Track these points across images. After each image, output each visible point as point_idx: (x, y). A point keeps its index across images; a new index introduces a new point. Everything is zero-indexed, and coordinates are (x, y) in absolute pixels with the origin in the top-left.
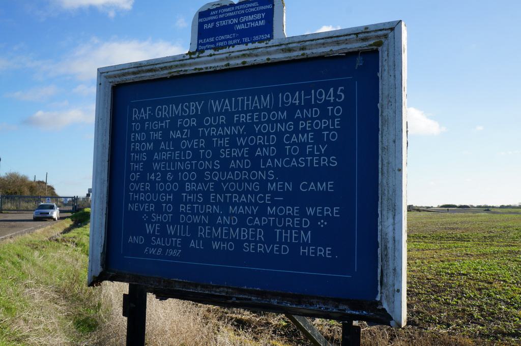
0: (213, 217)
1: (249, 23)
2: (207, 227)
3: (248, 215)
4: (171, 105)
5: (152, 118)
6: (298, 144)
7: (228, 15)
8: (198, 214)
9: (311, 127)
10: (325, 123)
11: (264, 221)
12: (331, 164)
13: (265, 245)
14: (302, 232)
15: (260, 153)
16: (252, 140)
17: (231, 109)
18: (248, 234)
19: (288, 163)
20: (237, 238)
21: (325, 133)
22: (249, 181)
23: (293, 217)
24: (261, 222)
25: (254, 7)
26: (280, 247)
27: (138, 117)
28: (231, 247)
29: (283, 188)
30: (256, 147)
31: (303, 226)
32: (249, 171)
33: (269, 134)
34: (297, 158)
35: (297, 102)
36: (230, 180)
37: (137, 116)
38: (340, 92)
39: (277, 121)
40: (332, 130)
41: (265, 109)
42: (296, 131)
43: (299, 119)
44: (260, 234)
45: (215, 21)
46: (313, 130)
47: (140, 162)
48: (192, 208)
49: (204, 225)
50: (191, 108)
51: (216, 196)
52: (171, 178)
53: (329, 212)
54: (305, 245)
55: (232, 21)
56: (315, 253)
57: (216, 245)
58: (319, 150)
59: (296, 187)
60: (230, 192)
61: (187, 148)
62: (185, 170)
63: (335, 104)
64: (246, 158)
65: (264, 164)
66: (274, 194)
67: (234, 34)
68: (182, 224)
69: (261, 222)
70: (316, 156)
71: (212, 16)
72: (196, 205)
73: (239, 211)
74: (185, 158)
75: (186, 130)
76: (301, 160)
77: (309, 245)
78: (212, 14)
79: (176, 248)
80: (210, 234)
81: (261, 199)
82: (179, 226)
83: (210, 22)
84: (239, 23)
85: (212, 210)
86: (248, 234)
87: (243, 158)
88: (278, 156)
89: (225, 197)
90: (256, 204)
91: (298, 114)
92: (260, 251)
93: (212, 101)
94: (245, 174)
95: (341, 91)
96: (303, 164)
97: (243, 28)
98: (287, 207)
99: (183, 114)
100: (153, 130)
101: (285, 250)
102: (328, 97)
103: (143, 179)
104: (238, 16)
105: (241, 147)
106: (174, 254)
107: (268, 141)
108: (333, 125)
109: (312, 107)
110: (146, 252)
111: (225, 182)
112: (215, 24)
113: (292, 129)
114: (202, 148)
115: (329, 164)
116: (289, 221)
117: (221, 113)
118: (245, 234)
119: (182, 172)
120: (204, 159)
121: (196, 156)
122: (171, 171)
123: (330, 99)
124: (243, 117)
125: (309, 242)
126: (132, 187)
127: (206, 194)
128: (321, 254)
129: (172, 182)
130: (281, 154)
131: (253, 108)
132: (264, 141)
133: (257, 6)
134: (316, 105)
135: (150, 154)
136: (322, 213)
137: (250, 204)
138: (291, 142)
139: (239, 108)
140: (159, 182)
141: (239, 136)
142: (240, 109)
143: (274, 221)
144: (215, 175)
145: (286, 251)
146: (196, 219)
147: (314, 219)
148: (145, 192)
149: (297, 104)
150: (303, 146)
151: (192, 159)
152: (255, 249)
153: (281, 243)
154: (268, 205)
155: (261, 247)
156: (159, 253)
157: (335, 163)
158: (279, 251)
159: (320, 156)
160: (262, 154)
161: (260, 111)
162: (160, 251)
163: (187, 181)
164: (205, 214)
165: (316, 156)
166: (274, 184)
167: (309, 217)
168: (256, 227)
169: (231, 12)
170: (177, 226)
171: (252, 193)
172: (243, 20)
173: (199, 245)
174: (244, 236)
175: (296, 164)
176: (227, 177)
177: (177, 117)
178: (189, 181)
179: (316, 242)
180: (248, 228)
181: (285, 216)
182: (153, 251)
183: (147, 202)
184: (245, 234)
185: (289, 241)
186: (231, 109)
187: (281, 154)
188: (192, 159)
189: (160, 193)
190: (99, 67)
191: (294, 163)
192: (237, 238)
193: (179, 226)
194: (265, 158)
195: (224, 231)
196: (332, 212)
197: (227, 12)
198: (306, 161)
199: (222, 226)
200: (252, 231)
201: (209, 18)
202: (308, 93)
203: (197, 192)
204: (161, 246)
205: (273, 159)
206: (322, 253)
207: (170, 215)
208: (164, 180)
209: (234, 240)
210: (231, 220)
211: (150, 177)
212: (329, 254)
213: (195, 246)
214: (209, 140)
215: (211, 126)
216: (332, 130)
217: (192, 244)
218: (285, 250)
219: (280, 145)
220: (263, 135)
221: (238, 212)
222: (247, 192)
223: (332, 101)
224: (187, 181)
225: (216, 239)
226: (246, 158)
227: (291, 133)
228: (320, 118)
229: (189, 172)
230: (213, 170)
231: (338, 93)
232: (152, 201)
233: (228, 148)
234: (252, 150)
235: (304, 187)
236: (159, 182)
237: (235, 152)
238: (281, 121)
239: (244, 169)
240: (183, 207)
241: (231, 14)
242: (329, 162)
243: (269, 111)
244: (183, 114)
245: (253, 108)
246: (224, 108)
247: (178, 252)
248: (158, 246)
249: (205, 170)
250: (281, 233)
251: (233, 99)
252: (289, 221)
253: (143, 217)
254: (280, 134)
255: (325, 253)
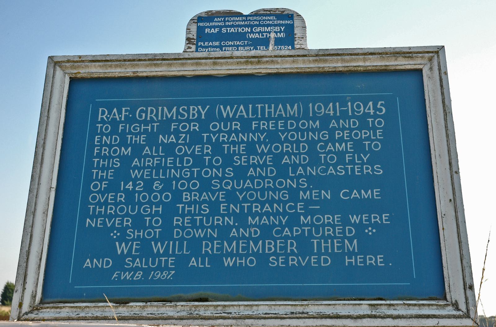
0: (224, 232)
1: (265, 34)
2: (215, 242)
3: (275, 225)
4: (160, 108)
5: (130, 120)
6: (335, 153)
7: (237, 23)
8: (202, 227)
9: (350, 136)
10: (365, 133)
11: (296, 231)
12: (338, 173)
13: (300, 257)
14: (346, 241)
15: (288, 161)
16: (277, 148)
17: (248, 115)
18: (275, 246)
19: (325, 171)
20: (261, 252)
21: (367, 143)
22: (274, 190)
23: (334, 226)
24: (292, 233)
25: (271, 20)
26: (319, 259)
27: (108, 118)
28: (251, 262)
29: (320, 196)
30: (282, 155)
31: (347, 235)
32: (274, 179)
33: (298, 142)
34: (335, 166)
35: (332, 113)
36: (248, 189)
37: (106, 117)
38: (380, 106)
39: (308, 130)
40: (374, 140)
41: (292, 117)
42: (332, 140)
43: (334, 129)
44: (292, 244)
45: (221, 27)
46: (352, 140)
47: (108, 168)
48: (193, 222)
49: (212, 239)
50: (191, 112)
51: (228, 207)
52: (161, 187)
53: (378, 220)
54: (351, 254)
55: (243, 30)
56: (365, 262)
57: (229, 262)
58: (360, 158)
59: (335, 195)
60: (247, 201)
61: (186, 154)
62: (181, 178)
63: (375, 116)
64: (270, 166)
65: (294, 171)
66: (308, 202)
67: (246, 42)
68: (177, 239)
69: (292, 233)
70: (358, 164)
71: (216, 22)
72: (198, 218)
73: (262, 222)
74: (183, 164)
75: (184, 135)
76: (228, 170)
77: (356, 255)
78: (216, 19)
79: (167, 268)
80: (342, 247)
81: (290, 208)
82: (171, 243)
83: (214, 27)
84: (252, 32)
85: (223, 222)
86: (275, 246)
87: (265, 165)
88: (311, 164)
89: (242, 208)
90: (284, 214)
91: (333, 124)
92: (371, 264)
93: (222, 107)
94: (269, 182)
95: (382, 105)
96: (342, 172)
97: (257, 38)
98: (326, 216)
99: (179, 117)
100: (130, 133)
101: (326, 261)
102: (368, 110)
103: (113, 187)
104: (252, 26)
105: (262, 154)
106: (164, 277)
107: (298, 148)
108: (375, 135)
109: (350, 118)
110: (115, 278)
111: (241, 191)
112: (221, 30)
113: (327, 138)
114: (208, 154)
115: (373, 172)
116: (328, 230)
117: (234, 119)
118: (271, 246)
119: (178, 180)
120: (211, 166)
121: (199, 161)
122: (159, 179)
123: (329, 112)
124: (264, 124)
125: (356, 251)
126: (94, 198)
127: (214, 207)
128: (372, 263)
129: (161, 192)
130: (315, 161)
131: (276, 116)
132: (292, 149)
133: (274, 20)
134: (354, 116)
135: (126, 161)
136: (369, 220)
137: (276, 214)
138: (327, 151)
139: (258, 115)
140: (140, 193)
141: (260, 143)
142: (259, 116)
143: (310, 231)
144: (228, 183)
145: (326, 262)
146: (200, 233)
147: (360, 227)
148: (116, 204)
149: (332, 115)
150: (341, 155)
151: (193, 166)
152: (286, 262)
153: (319, 254)
154: (301, 214)
155: (293, 260)
156: (138, 277)
157: (380, 172)
158: (319, 262)
159: (363, 164)
160: (291, 162)
161: (286, 119)
162: (139, 275)
163: (185, 191)
164: (213, 227)
165: (358, 164)
166: (308, 192)
167: (355, 225)
168: (287, 237)
169: (242, 21)
170: (169, 244)
171: (279, 202)
172: (258, 30)
173: (203, 263)
174: (270, 249)
175: (333, 172)
176: (244, 185)
177: (170, 120)
178: (189, 190)
179: (363, 250)
180: (275, 240)
181: (323, 225)
182: (128, 276)
183: (120, 216)
184: (271, 246)
185: (330, 251)
186: (248, 115)
187: (315, 161)
188: (193, 166)
189: (140, 204)
190: (50, 56)
191: (331, 170)
192: (261, 252)
193: (171, 243)
194: (295, 167)
195: (241, 245)
196: (381, 219)
197: (237, 21)
198: (346, 170)
199: (238, 239)
200: (217, 244)
201: (213, 24)
202: (343, 104)
203: (201, 203)
204: (141, 269)
205: (304, 167)
206: (373, 262)
207: (158, 230)
208: (148, 187)
209: (254, 254)
210: (250, 233)
211: (125, 186)
212: (381, 262)
213: (198, 264)
214: (217, 148)
215: (220, 131)
216: (374, 140)
217: (193, 262)
218: (326, 261)
219: (312, 153)
220: (292, 143)
221: (260, 222)
222: (271, 202)
223: (332, 115)
224: (185, 191)
225: (231, 255)
226: (270, 166)
227: (326, 143)
228: (360, 128)
229: (189, 180)
230: (224, 177)
231: (379, 106)
232: (127, 215)
233: (244, 155)
234: (277, 158)
235: (345, 194)
236: (140, 193)
237: (255, 160)
238: (313, 131)
239: (267, 177)
240: (178, 220)
241: (241, 23)
242: (373, 170)
243: (297, 120)
244: (179, 117)
245: (276, 116)
246: (238, 114)
247: (170, 273)
248: (136, 269)
249: (211, 178)
250: (319, 244)
251: (129, 108)
252: (328, 230)
253: (370, 233)
254: (312, 143)
255: (376, 262)
